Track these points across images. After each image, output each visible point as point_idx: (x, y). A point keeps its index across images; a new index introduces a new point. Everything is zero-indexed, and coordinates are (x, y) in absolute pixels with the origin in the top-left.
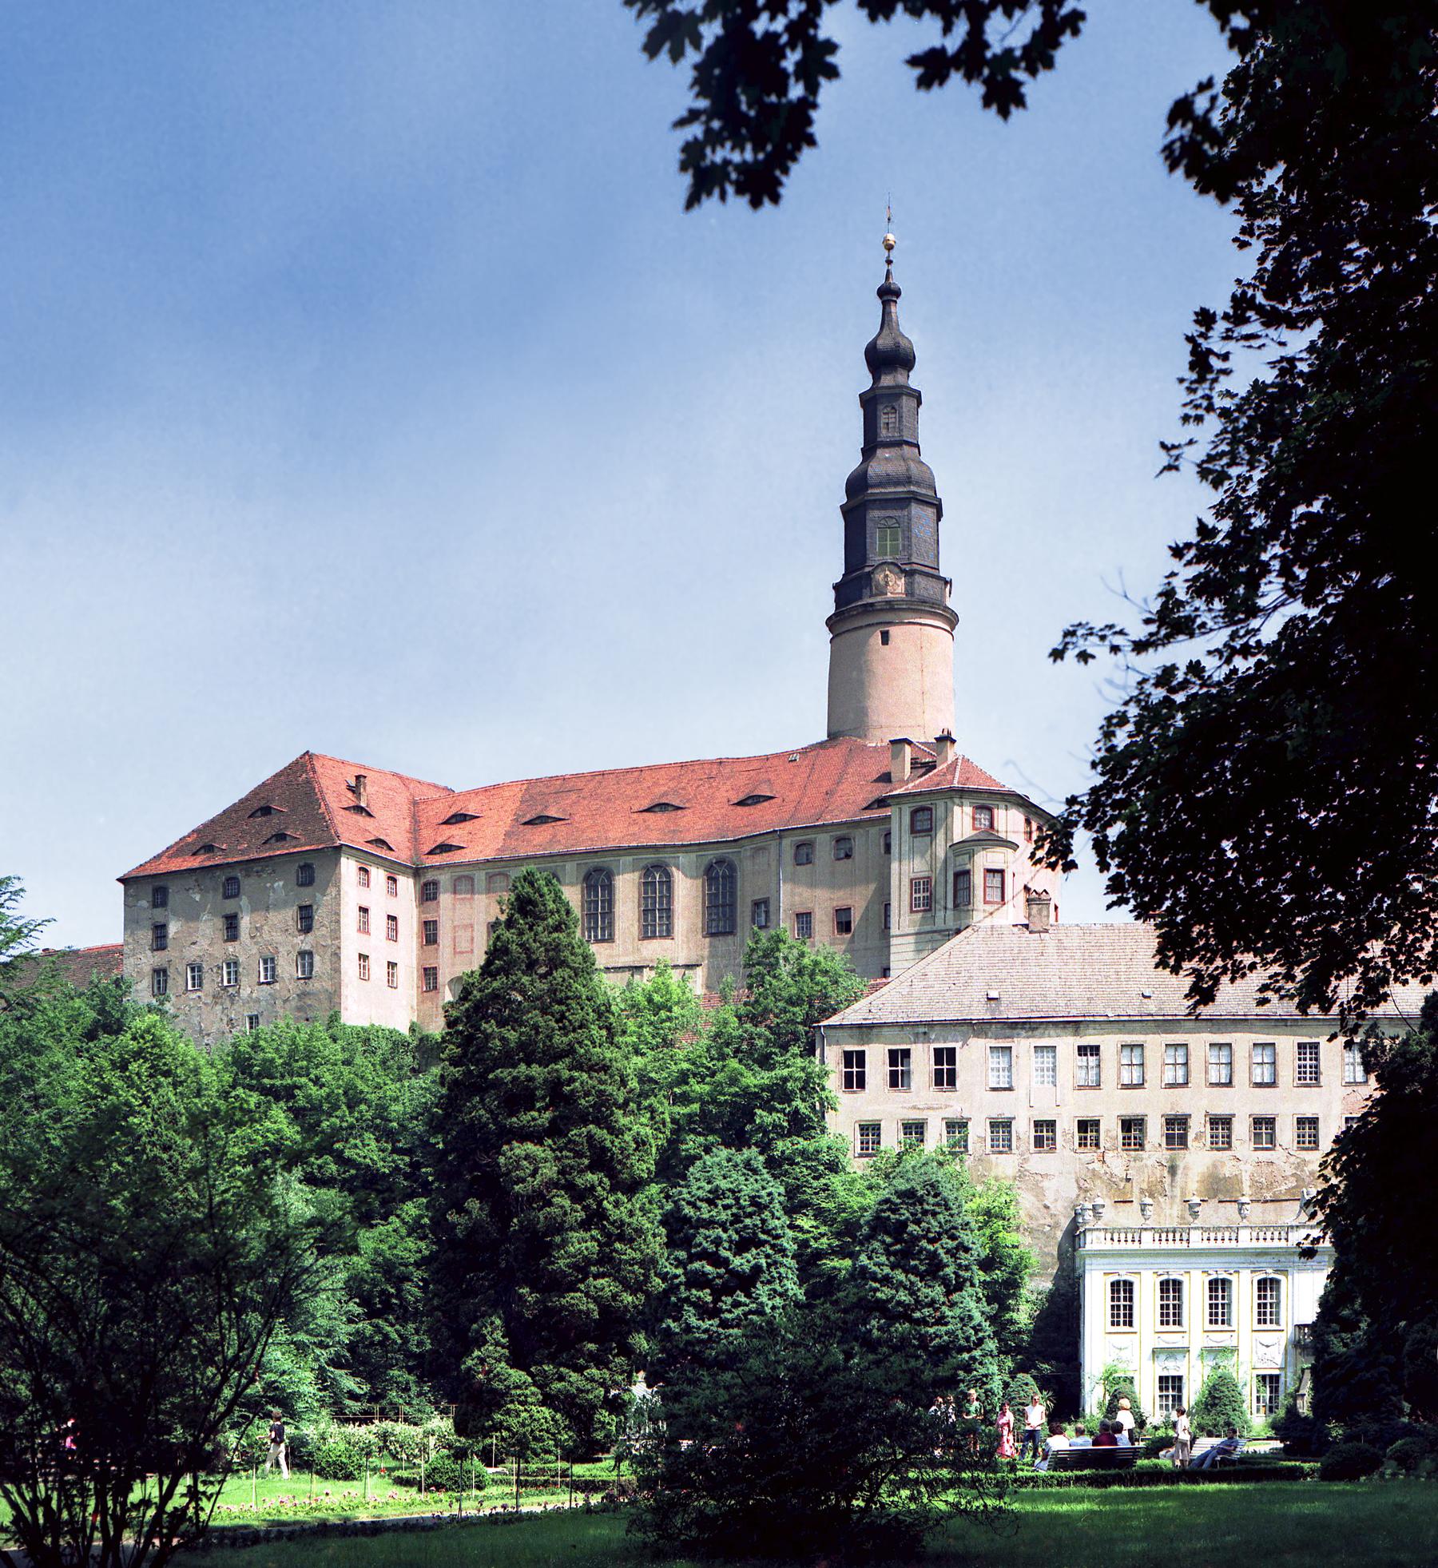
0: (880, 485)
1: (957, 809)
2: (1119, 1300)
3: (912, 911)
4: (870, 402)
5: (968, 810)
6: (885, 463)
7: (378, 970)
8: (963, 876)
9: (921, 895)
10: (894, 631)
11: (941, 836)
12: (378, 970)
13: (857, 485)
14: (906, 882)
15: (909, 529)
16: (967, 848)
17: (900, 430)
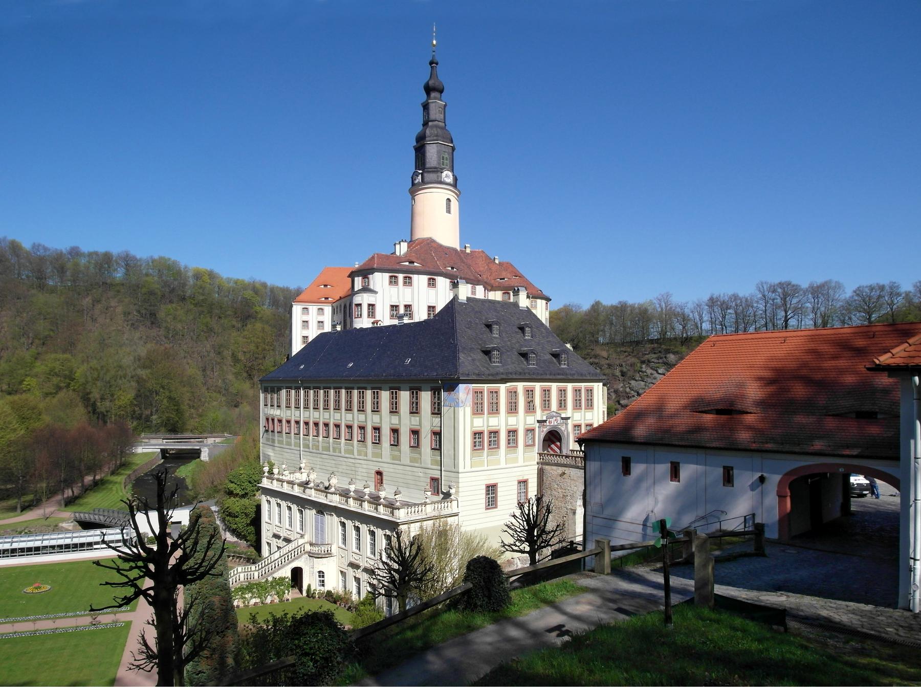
1: (356, 279)
5: (360, 278)
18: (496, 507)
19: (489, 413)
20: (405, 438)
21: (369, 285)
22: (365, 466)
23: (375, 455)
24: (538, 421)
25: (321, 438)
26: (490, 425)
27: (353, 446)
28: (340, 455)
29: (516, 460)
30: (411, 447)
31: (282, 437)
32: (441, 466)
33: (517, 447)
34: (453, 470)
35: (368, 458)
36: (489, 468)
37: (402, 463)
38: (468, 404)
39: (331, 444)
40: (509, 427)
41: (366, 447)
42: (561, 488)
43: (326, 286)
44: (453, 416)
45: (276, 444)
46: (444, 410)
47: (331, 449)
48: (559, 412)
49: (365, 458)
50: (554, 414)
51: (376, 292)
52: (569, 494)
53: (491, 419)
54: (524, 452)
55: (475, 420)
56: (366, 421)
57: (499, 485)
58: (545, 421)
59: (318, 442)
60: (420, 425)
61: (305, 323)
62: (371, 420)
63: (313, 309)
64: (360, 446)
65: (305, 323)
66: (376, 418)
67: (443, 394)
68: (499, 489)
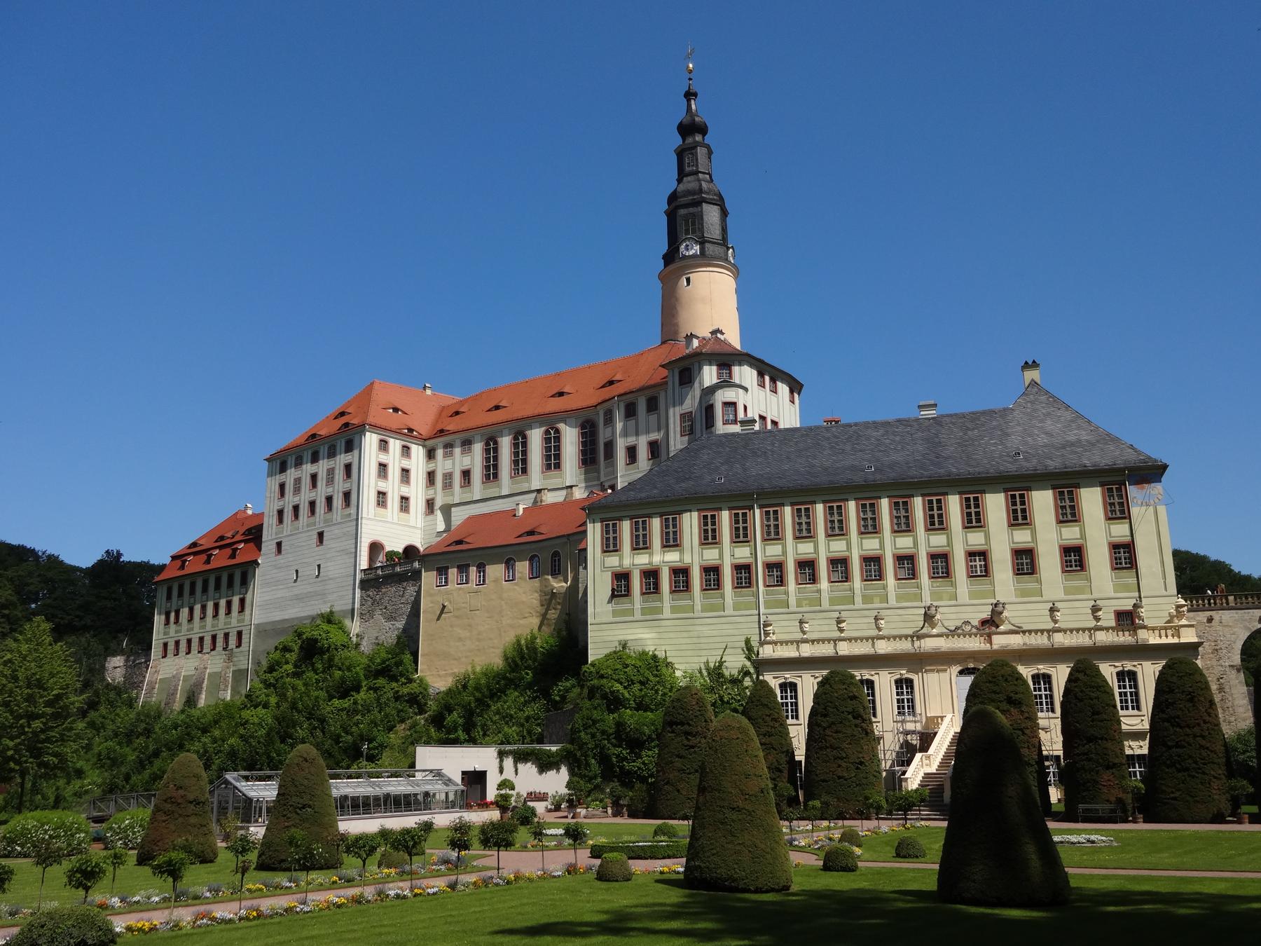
0: (684, 196)
2: (786, 698)
3: (682, 436)
4: (681, 153)
5: (714, 368)
6: (689, 184)
7: (393, 501)
8: (709, 410)
9: (687, 424)
10: (691, 276)
11: (696, 384)
12: (393, 501)
13: (673, 198)
14: (678, 418)
15: (702, 219)
16: (712, 390)
17: (697, 166)
20: (1050, 561)
21: (731, 376)
22: (953, 616)
23: (972, 595)
25: (824, 584)
27: (919, 587)
28: (885, 605)
30: (1064, 571)
31: (692, 599)
32: (1139, 591)
34: (1165, 593)
35: (960, 601)
37: (1045, 598)
39: (858, 591)
41: (954, 585)
42: (1209, 640)
43: (396, 410)
44: (1153, 519)
45: (667, 613)
46: (1135, 511)
47: (858, 599)
49: (953, 602)
51: (746, 389)
52: (1223, 647)
56: (950, 543)
59: (819, 591)
60: (1083, 535)
61: (383, 467)
62: (959, 541)
63: (395, 445)
64: (935, 585)
65: (383, 467)
66: (976, 539)
67: (1133, 491)
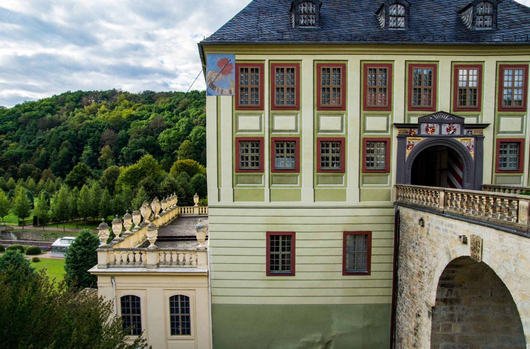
18: (293, 274)
19: (273, 107)
24: (398, 126)
26: (276, 128)
29: (342, 195)
33: (343, 170)
36: (273, 204)
38: (227, 91)
40: (320, 135)
48: (458, 113)
50: (446, 118)
53: (277, 119)
54: (361, 182)
55: (241, 118)
57: (297, 237)
58: (416, 126)
68: (298, 244)
